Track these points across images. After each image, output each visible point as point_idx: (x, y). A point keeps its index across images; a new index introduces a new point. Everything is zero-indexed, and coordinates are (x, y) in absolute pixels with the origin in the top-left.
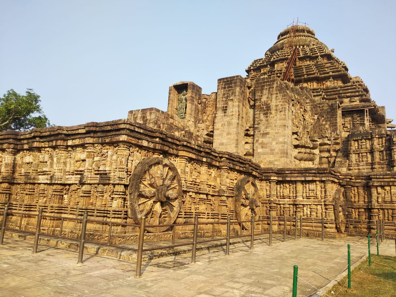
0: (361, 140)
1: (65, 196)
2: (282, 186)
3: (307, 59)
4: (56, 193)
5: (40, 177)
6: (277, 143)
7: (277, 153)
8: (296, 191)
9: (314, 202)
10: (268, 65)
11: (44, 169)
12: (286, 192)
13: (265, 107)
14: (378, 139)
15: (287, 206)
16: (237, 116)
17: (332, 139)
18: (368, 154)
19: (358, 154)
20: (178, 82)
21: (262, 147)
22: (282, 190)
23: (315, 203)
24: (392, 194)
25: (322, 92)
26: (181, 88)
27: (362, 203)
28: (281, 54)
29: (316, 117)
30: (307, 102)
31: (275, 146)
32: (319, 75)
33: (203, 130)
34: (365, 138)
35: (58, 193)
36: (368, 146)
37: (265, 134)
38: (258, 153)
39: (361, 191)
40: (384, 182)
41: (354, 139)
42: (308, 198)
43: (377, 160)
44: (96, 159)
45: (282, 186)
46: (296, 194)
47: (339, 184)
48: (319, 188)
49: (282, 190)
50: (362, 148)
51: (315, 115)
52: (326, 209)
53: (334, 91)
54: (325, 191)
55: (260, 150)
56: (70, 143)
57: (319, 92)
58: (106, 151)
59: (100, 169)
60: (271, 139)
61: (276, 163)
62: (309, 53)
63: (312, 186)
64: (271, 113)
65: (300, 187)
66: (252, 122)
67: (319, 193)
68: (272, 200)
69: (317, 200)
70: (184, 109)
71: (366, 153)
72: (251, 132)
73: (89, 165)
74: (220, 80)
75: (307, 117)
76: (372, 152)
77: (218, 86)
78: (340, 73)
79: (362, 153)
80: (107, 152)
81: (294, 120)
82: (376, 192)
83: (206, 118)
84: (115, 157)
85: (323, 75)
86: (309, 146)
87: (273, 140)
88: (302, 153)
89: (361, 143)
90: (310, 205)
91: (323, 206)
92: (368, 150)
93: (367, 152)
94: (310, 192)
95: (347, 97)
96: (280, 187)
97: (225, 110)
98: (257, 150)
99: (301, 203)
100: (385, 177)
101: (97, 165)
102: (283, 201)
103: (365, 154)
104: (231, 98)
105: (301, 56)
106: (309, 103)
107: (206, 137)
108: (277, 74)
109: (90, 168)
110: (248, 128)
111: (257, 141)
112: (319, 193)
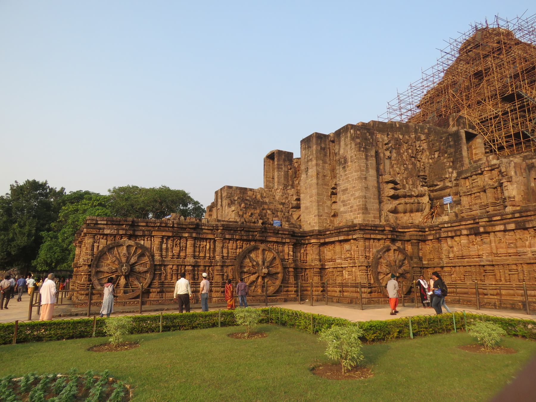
0: (471, 176)
7: (355, 210)
13: (343, 160)
14: (490, 172)
16: (316, 177)
17: (453, 180)
18: (482, 193)
19: (471, 194)
20: (267, 152)
21: (344, 205)
24: (463, 246)
26: (271, 157)
29: (436, 156)
30: (422, 139)
33: (292, 195)
34: (474, 173)
40: (451, 231)
41: (463, 176)
42: (345, 259)
50: (473, 187)
51: (436, 153)
55: (342, 209)
63: (347, 246)
64: (348, 166)
65: (338, 247)
71: (479, 192)
74: (302, 142)
77: (301, 147)
79: (474, 193)
81: (395, 166)
83: (297, 182)
86: (413, 193)
87: (352, 195)
88: (402, 204)
89: (473, 180)
93: (479, 191)
97: (307, 169)
99: (339, 266)
100: (453, 225)
103: (478, 194)
104: (311, 157)
106: (424, 140)
107: (295, 202)
110: (333, 186)
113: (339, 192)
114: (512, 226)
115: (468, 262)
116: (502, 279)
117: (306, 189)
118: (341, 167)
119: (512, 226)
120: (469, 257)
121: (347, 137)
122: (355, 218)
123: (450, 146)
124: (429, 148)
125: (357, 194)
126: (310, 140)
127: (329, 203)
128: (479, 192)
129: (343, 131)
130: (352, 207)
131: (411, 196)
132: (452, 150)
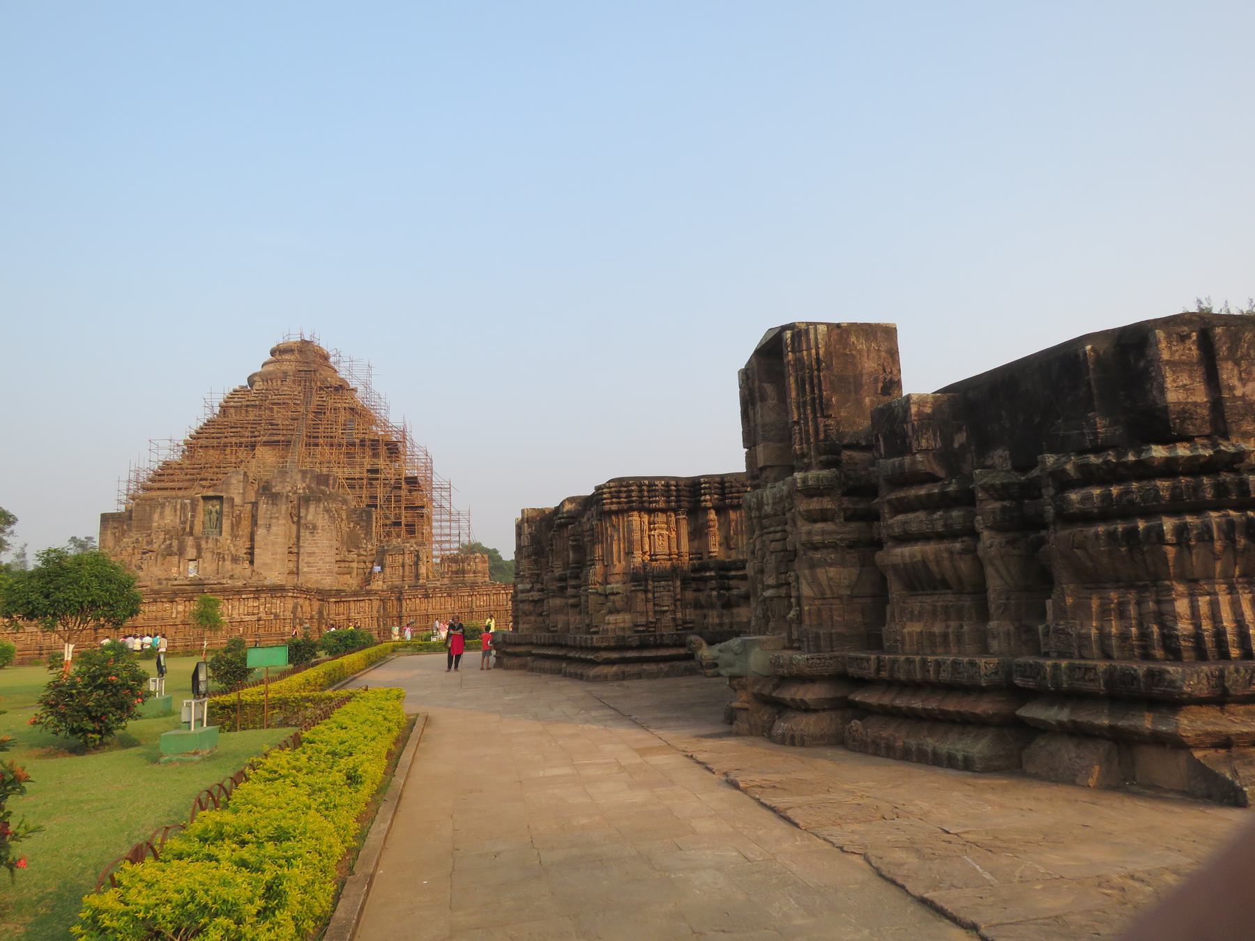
12: (341, 610)
21: (308, 567)
27: (395, 613)
29: (352, 525)
36: (400, 560)
37: (311, 554)
38: (304, 572)
39: (395, 603)
43: (407, 573)
47: (381, 600)
55: (305, 570)
56: (244, 596)
61: (323, 581)
63: (362, 604)
65: (352, 605)
66: (296, 540)
67: (367, 609)
72: (295, 550)
75: (343, 525)
76: (403, 566)
87: (320, 559)
111: (303, 560)
112: (367, 609)
113: (303, 553)
114: (445, 595)
117: (265, 544)
118: (307, 532)
119: (445, 595)
121: (319, 507)
123: (362, 520)
124: (347, 518)
125: (327, 559)
126: (277, 497)
129: (313, 500)
132: (365, 524)
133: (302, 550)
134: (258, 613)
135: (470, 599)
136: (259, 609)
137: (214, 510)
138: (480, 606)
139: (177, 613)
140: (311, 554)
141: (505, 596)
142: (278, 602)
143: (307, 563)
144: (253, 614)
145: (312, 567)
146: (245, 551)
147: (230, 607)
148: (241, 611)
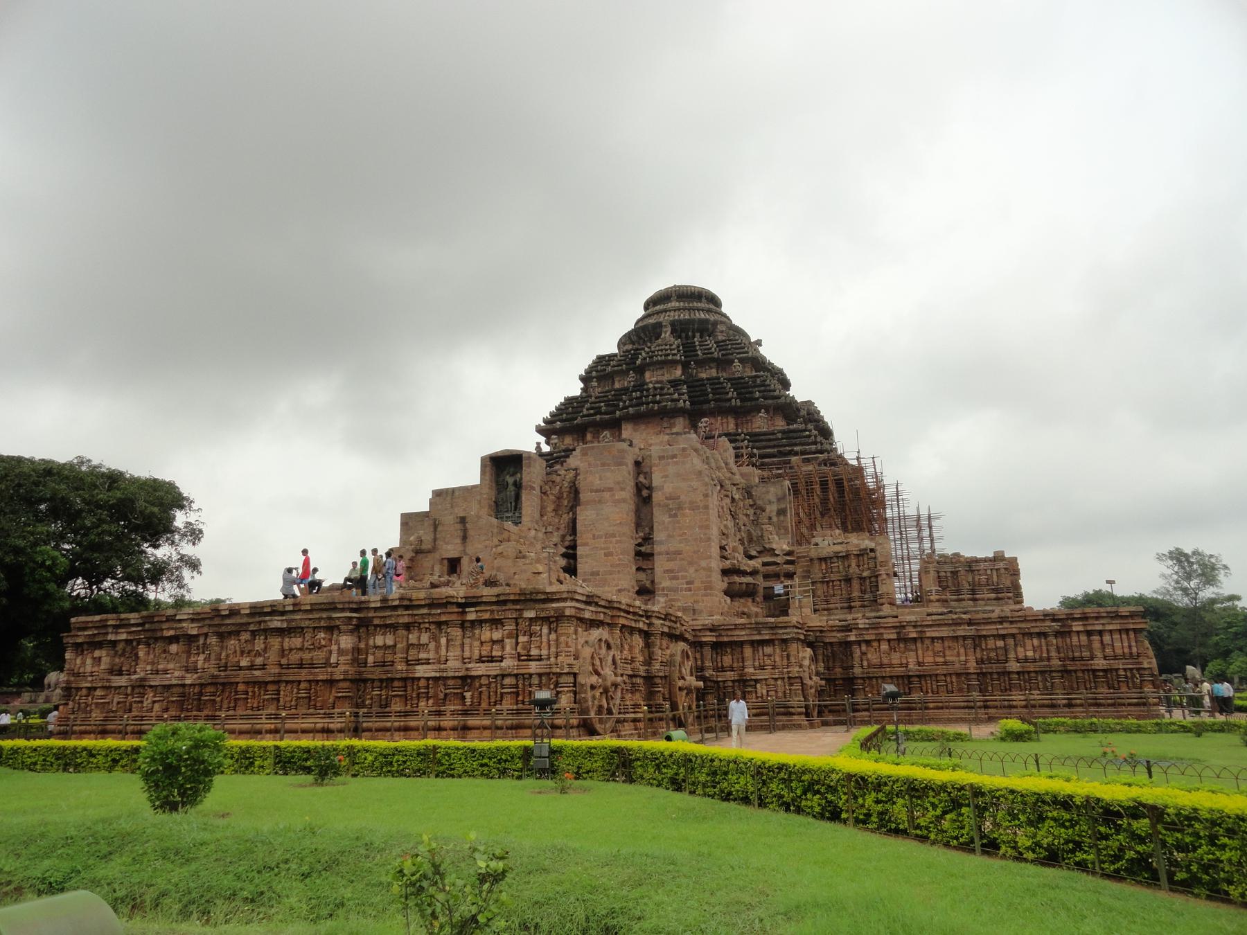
1: (468, 695)
2: (719, 651)
3: (712, 365)
4: (456, 691)
5: (418, 667)
6: (696, 570)
7: (699, 589)
8: (743, 658)
9: (772, 674)
10: (631, 372)
11: (423, 655)
15: (730, 684)
18: (843, 583)
19: (828, 582)
22: (719, 658)
23: (774, 676)
25: (749, 441)
28: (658, 351)
31: (693, 575)
32: (739, 403)
35: (459, 691)
38: (663, 589)
42: (762, 668)
43: (856, 594)
44: (522, 639)
45: (719, 651)
46: (743, 662)
48: (778, 651)
49: (719, 658)
50: (832, 573)
52: (791, 684)
53: (770, 440)
54: (788, 656)
55: (666, 583)
56: (471, 616)
57: (743, 441)
58: (538, 628)
59: (532, 653)
60: (686, 563)
62: (716, 353)
63: (768, 650)
67: (778, 659)
68: (707, 675)
69: (777, 671)
70: (513, 504)
73: (512, 649)
76: (848, 580)
78: (779, 401)
79: (833, 581)
80: (541, 630)
82: (858, 650)
84: (553, 636)
85: (749, 404)
87: (691, 564)
90: (766, 679)
91: (786, 680)
92: (843, 576)
94: (766, 658)
95: (796, 454)
96: (717, 654)
98: (661, 583)
99: (753, 677)
101: (524, 648)
102: (721, 676)
103: (838, 583)
105: (700, 358)
108: (654, 395)
109: (514, 652)
110: (640, 540)
112: (778, 659)
115: (890, 672)
116: (930, 691)
120: (891, 666)
122: (697, 602)
127: (634, 568)
128: (840, 581)
130: (688, 583)
131: (744, 573)
133: (657, 549)
134: (501, 659)
135: (1000, 643)
136: (503, 648)
137: (510, 480)
138: (1026, 660)
139: (341, 652)
140: (674, 555)
141: (1084, 638)
142: (545, 630)
143: (665, 572)
144: (491, 659)
145: (676, 578)
146: (564, 550)
147: (443, 641)
148: (467, 654)
